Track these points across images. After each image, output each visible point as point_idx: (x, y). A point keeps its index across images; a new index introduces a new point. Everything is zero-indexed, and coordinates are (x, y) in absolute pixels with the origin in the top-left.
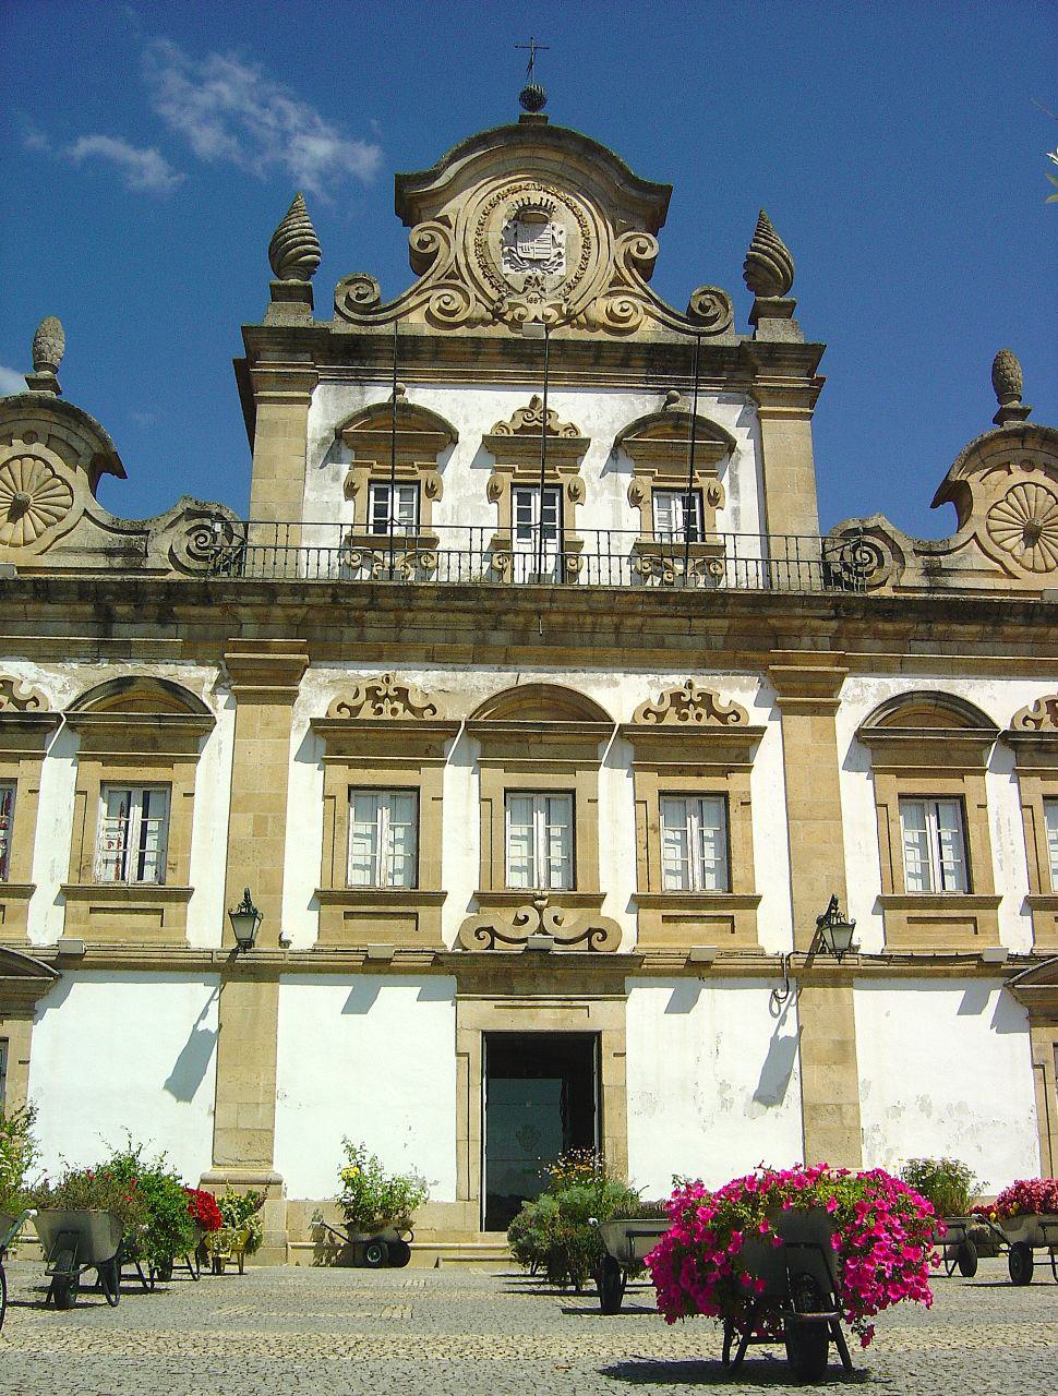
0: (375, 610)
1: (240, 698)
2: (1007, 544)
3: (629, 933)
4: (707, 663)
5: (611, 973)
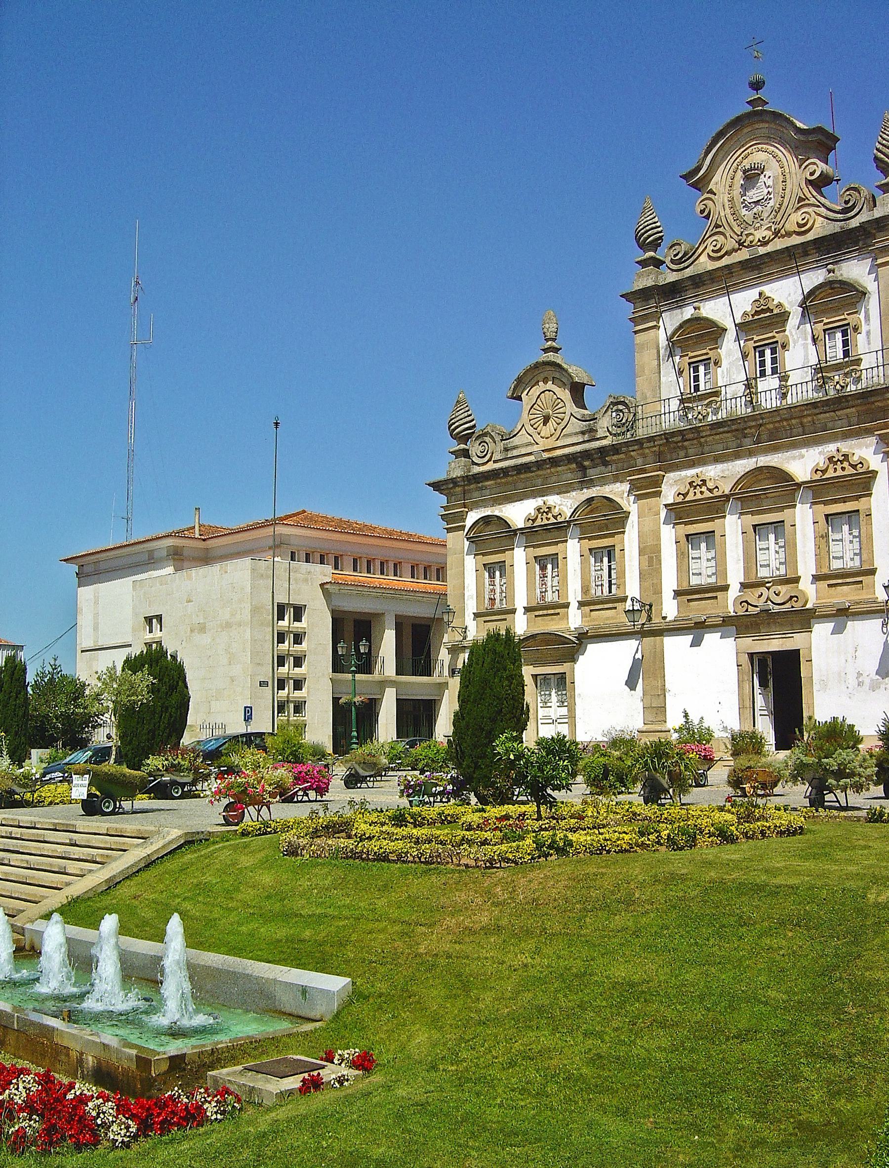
1: (639, 497)
3: (811, 593)
4: (846, 436)
5: (803, 619)
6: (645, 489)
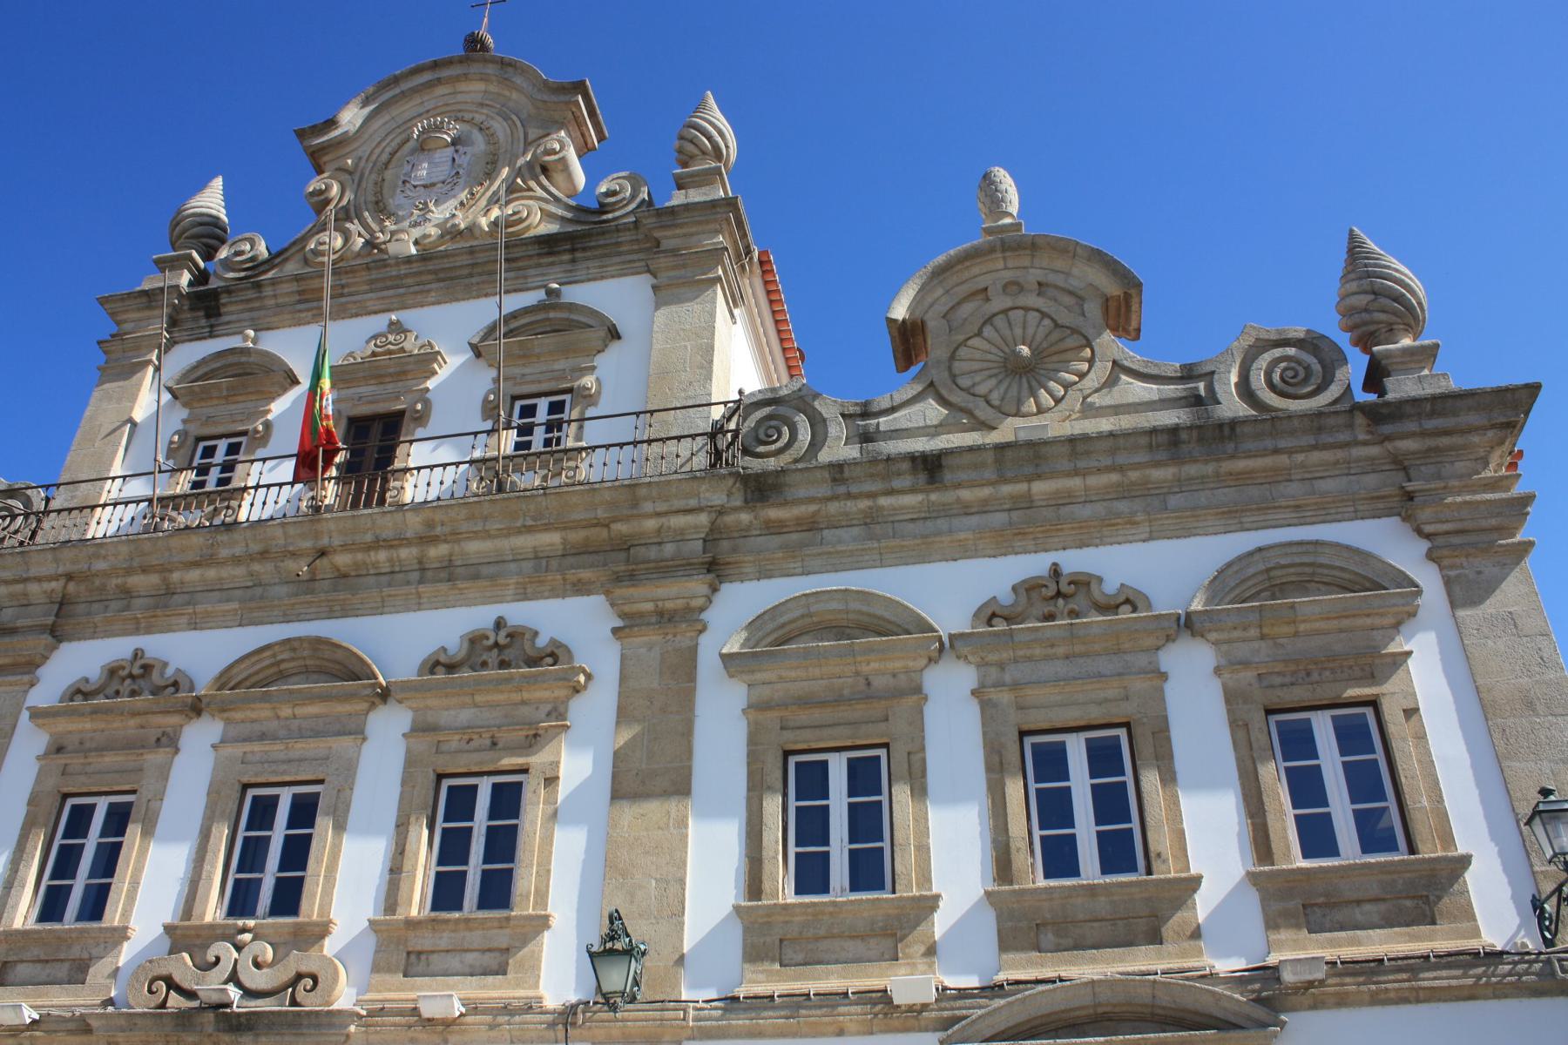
2: (982, 389)
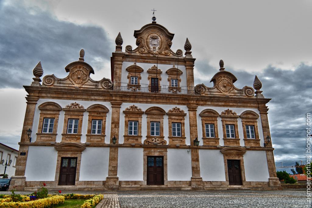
0: (134, 95)
2: (221, 88)
4: (179, 104)
6: (116, 105)
